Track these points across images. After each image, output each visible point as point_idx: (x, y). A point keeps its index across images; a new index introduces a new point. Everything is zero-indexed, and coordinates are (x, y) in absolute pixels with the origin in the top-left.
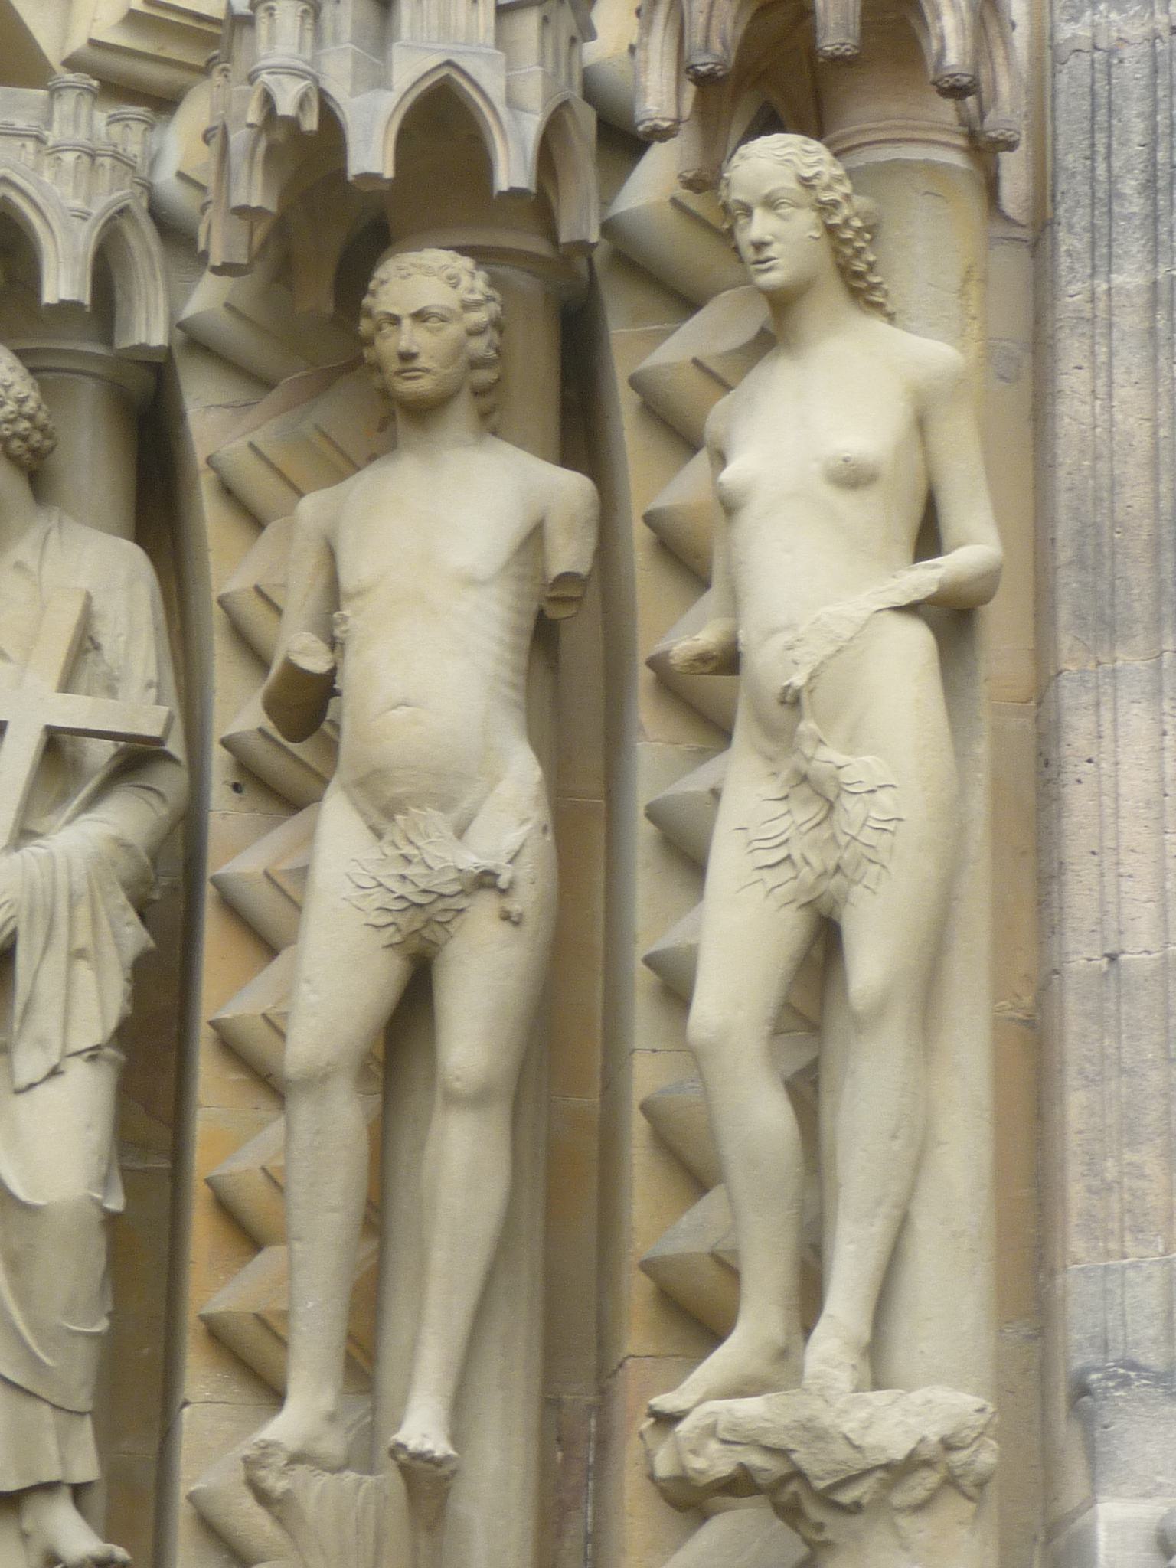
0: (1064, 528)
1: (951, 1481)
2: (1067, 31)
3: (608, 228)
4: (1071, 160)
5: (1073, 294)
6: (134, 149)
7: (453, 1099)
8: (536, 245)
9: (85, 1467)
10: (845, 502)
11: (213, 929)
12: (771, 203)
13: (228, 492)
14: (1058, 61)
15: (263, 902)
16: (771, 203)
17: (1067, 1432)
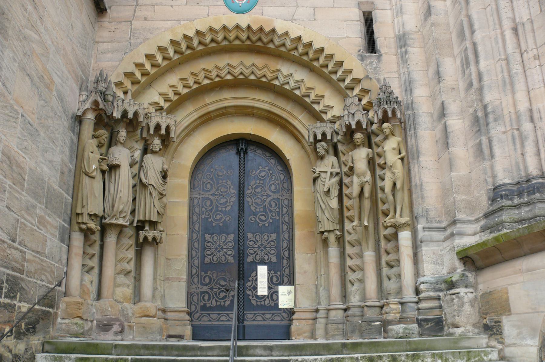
0: (409, 151)
1: (407, 225)
2: (406, 113)
3: (371, 130)
4: (407, 123)
5: (408, 133)
6: (333, 127)
7: (366, 198)
8: (366, 132)
9: (338, 228)
10: (394, 151)
11: (344, 187)
12: (386, 128)
13: (342, 152)
14: (405, 115)
15: (348, 184)
16: (386, 128)
17: (415, 220)
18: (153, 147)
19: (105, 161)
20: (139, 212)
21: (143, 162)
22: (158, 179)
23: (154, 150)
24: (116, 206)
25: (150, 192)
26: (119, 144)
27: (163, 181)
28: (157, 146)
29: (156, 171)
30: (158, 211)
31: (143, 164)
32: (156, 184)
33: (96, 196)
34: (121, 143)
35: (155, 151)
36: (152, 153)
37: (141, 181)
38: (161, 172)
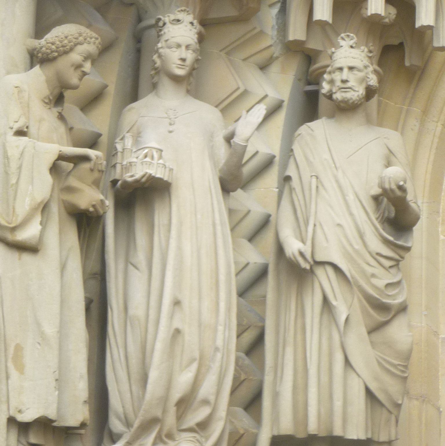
18: (332, 82)
19: (86, 166)
20: (276, 396)
21: (292, 160)
22: (361, 236)
23: (338, 96)
24: (153, 375)
25: (325, 300)
26: (166, 85)
27: (386, 242)
28: (353, 79)
29: (351, 197)
30: (369, 392)
31: (291, 171)
32: (351, 260)
33: (42, 334)
34: (176, 79)
35: (345, 101)
36: (331, 116)
37: (280, 250)
38: (376, 199)
